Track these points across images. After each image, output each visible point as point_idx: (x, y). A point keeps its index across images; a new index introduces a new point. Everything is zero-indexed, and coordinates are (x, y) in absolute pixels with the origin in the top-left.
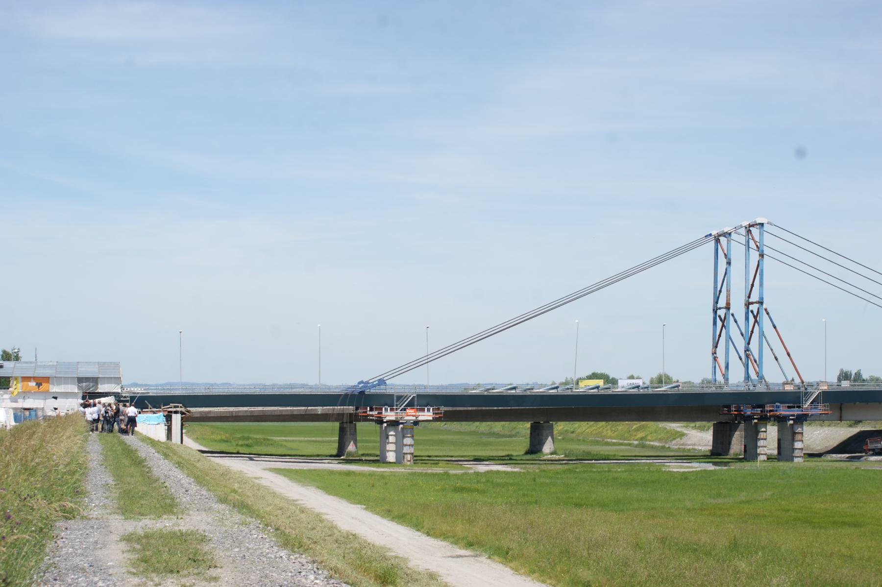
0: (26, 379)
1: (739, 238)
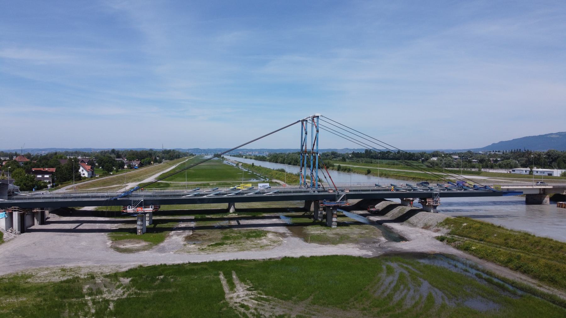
1: (310, 122)
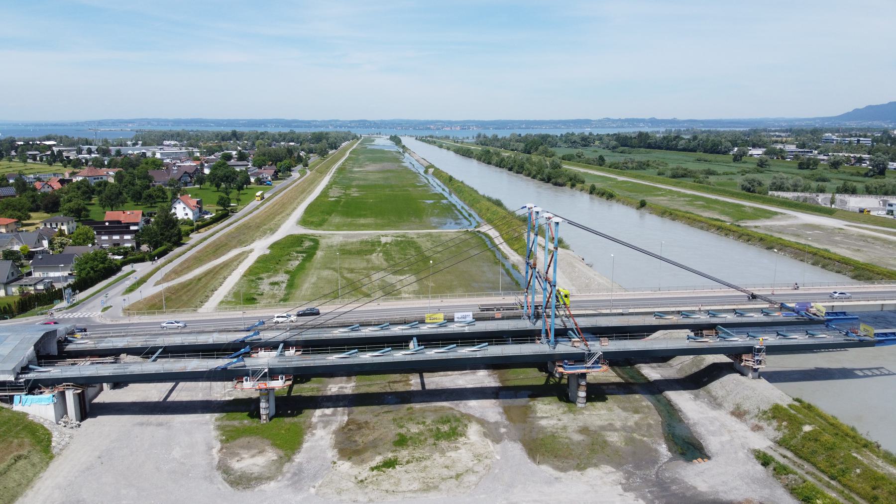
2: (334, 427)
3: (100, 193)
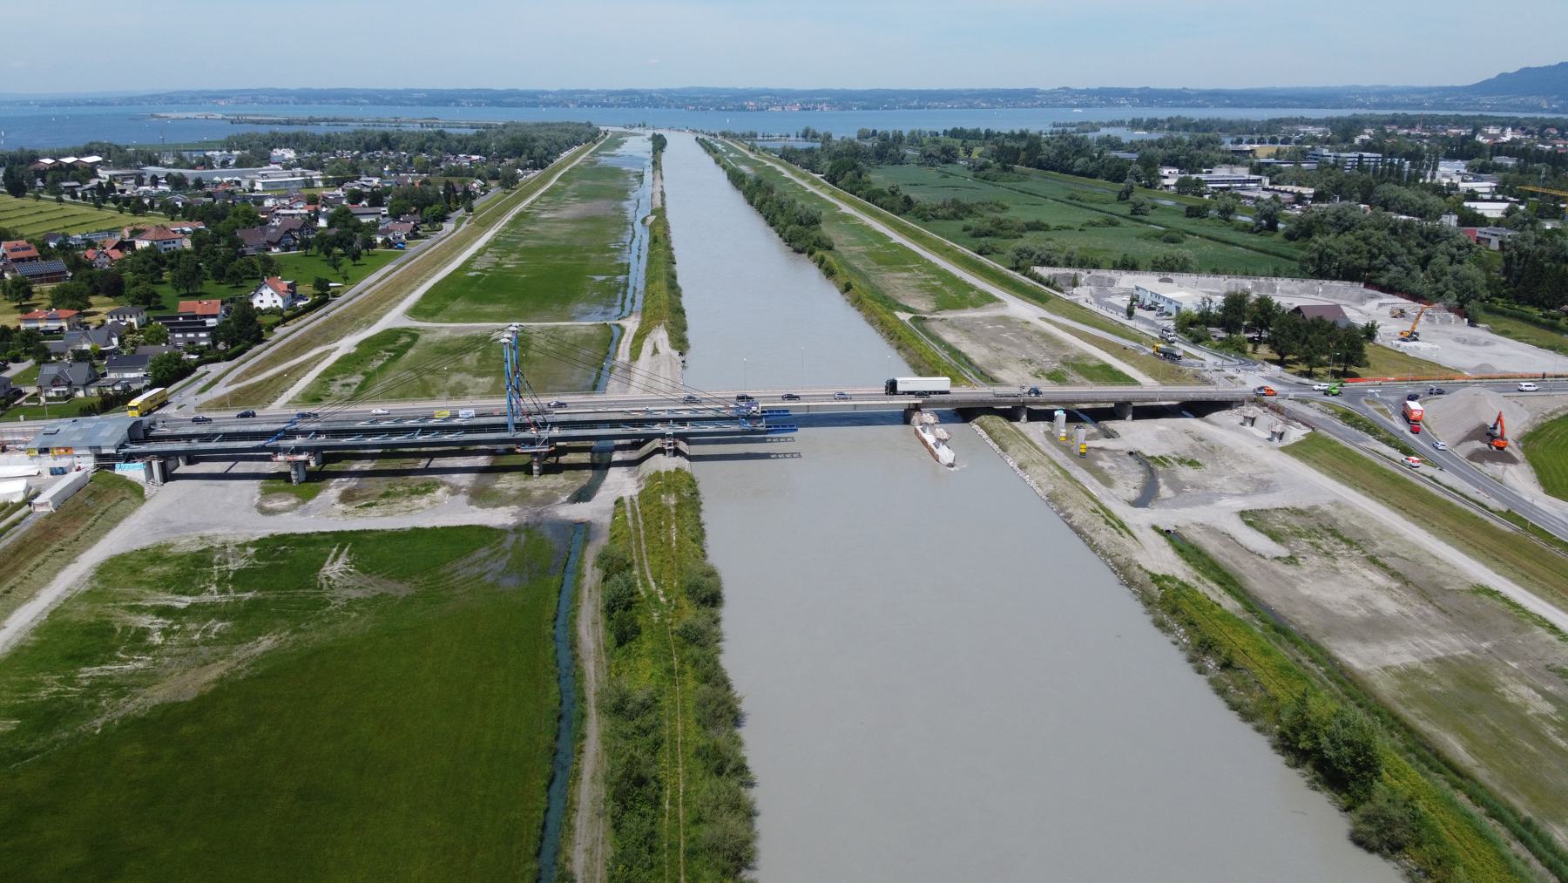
0: (59, 448)
2: (343, 488)
3: (172, 267)
